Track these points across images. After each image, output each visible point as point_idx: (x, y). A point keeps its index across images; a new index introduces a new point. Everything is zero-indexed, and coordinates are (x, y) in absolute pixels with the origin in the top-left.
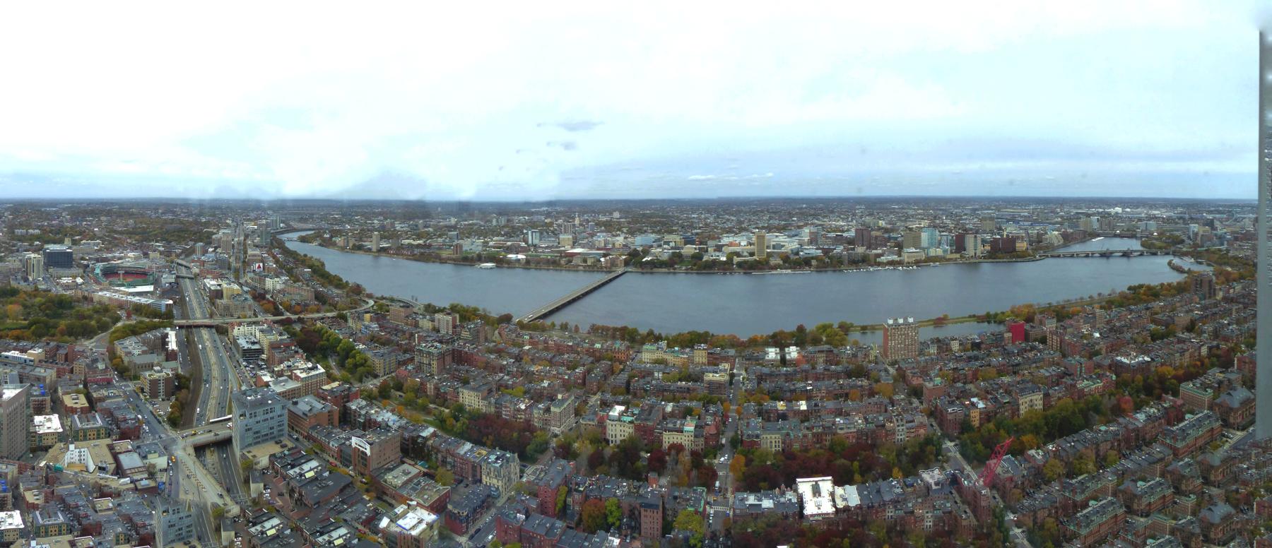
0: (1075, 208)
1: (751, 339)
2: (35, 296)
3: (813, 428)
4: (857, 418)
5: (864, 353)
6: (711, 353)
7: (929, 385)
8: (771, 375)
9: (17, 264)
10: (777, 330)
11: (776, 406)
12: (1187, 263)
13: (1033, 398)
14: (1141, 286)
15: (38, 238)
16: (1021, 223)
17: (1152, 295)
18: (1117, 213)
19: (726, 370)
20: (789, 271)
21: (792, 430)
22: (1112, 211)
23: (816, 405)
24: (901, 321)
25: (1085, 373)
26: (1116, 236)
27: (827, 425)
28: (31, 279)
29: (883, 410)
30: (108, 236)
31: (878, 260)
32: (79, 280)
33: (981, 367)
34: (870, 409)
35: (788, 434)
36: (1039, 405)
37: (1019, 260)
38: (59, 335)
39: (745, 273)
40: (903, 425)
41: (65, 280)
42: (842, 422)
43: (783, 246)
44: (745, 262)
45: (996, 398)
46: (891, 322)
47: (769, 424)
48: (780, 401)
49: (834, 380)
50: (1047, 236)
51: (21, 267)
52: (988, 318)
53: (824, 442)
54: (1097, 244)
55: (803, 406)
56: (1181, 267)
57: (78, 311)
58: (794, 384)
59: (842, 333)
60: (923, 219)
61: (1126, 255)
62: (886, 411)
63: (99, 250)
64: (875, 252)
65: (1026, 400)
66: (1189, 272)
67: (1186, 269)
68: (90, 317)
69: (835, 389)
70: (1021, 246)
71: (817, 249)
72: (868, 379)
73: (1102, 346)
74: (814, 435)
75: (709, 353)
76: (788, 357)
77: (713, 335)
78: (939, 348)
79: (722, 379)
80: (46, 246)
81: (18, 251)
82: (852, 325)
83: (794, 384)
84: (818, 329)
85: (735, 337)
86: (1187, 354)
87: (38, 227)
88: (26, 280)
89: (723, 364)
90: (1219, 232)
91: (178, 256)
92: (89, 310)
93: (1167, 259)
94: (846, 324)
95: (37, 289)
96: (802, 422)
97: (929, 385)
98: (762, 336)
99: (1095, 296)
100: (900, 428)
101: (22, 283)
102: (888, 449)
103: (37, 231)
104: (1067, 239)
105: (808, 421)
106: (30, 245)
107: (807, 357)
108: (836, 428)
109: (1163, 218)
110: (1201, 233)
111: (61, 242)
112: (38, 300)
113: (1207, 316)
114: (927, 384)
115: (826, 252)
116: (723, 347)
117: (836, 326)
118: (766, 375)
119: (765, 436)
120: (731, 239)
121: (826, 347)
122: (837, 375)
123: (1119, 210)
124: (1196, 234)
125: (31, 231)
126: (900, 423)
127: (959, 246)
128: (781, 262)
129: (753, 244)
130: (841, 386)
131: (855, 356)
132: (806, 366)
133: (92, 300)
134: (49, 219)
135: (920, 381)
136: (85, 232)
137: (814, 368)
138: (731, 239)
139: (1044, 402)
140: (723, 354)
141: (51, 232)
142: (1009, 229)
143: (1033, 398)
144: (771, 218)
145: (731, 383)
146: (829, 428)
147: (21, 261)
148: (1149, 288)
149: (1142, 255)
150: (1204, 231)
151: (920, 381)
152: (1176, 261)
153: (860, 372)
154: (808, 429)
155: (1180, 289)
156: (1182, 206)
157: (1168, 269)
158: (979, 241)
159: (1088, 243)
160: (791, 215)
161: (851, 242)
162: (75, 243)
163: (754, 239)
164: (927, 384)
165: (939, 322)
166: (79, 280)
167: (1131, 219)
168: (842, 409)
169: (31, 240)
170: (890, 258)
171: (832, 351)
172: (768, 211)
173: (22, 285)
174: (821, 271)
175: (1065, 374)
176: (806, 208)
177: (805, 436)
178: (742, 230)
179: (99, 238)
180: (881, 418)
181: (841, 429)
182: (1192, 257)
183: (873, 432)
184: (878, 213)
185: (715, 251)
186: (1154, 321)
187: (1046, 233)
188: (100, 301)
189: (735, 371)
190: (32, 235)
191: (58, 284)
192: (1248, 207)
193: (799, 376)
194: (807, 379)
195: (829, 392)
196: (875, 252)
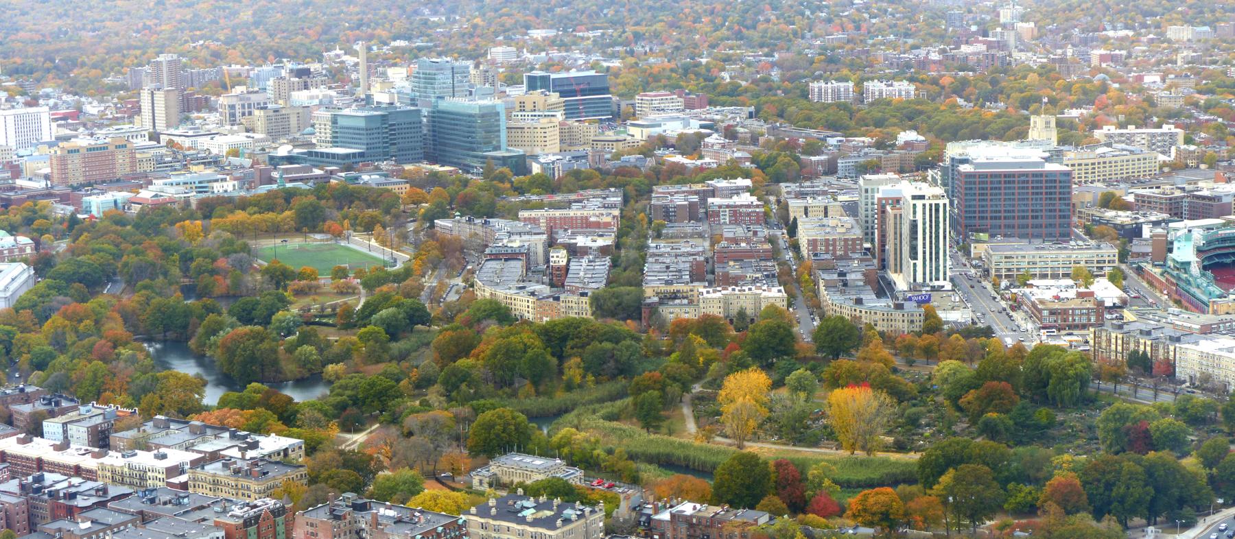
2: (930, 354)
9: (842, 226)
15: (910, 116)
28: (901, 282)
30: (1207, 108)
32: (1107, 292)
38: (1053, 508)
41: (1043, 291)
51: (858, 233)
57: (1122, 416)
63: (1176, 167)
68: (1175, 442)
80: (953, 150)
81: (831, 169)
87: (903, 71)
88: (883, 288)
92: (1164, 411)
95: (932, 325)
101: (870, 298)
103: (903, 89)
106: (879, 145)
111: (1015, 131)
112: (947, 366)
125: (875, 87)
133: (1169, 369)
134: (942, 37)
136: (1104, 89)
141: (960, 88)
147: (851, 209)
162: (1068, 134)
166: (1107, 292)
169: (879, 123)
173: (874, 310)
179: (1170, 116)
188: (1206, 378)
190: (880, 102)
191: (1017, 304)
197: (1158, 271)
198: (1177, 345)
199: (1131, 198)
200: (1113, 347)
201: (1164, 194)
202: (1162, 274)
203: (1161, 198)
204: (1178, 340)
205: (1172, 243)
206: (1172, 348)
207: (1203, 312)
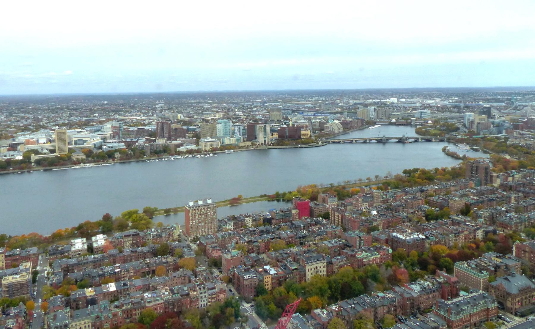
0: (354, 99)
1: (54, 234)
3: (123, 305)
4: (164, 291)
5: (168, 233)
6: (10, 256)
7: (227, 256)
8: (79, 264)
10: (83, 221)
11: (84, 294)
12: (463, 150)
13: (317, 265)
14: (416, 170)
16: (305, 113)
17: (426, 179)
18: (392, 103)
19: (27, 270)
20: (93, 165)
21: (101, 312)
22: (388, 101)
23: (125, 285)
24: (200, 203)
25: (364, 246)
26: (391, 124)
27: (135, 300)
29: (187, 281)
31: (178, 149)
33: (272, 239)
34: (175, 281)
35: (98, 317)
36: (323, 271)
37: (304, 146)
39: (45, 170)
40: (205, 293)
42: (150, 296)
43: (85, 141)
44: (45, 159)
45: (286, 265)
46: (191, 204)
47: (77, 312)
48: (88, 287)
49: (141, 260)
50: (328, 125)
52: (277, 197)
53: (134, 317)
54: (374, 132)
55: (112, 287)
56: (456, 154)
58: (102, 269)
59: (146, 217)
60: (218, 112)
61: (401, 141)
62: (190, 282)
64: (175, 142)
65: (312, 267)
66: (464, 158)
67: (461, 156)
69: (142, 268)
70: (306, 133)
71: (120, 142)
72: (172, 256)
73: (379, 222)
74: (124, 312)
75: (6, 256)
76: (95, 245)
77: (10, 237)
78: (235, 224)
79: (24, 279)
82: (156, 210)
83: (102, 269)
84: (124, 215)
85: (36, 235)
86: (462, 236)
89: (24, 264)
90: (497, 120)
93: (442, 145)
94: (150, 209)
96: (112, 302)
97: (227, 256)
98: (67, 229)
99: (373, 178)
100: (203, 295)
102: (192, 315)
104: (347, 127)
105: (118, 300)
107: (114, 242)
108: (145, 302)
109: (438, 107)
110: (477, 121)
113: (482, 202)
114: (225, 255)
115: (129, 145)
116: (22, 247)
117: (141, 211)
118: (73, 265)
119: (74, 324)
120: (27, 137)
121: (132, 231)
122: (144, 256)
123: (394, 100)
124: (472, 122)
126: (203, 291)
127: (250, 134)
128: (84, 157)
129: (54, 141)
130: (148, 265)
131: (160, 236)
132: (114, 251)
135: (219, 253)
137: (121, 252)
138: (27, 137)
139: (327, 269)
140: (24, 254)
142: (294, 119)
143: (317, 265)
144: (71, 115)
145: (34, 281)
146: (138, 303)
148: (424, 172)
149: (416, 141)
150: (480, 119)
151: (219, 253)
152: (451, 148)
153: (166, 251)
154: (118, 307)
155: (455, 174)
156: (457, 95)
157: (442, 155)
158: (268, 130)
159: (366, 130)
160: (92, 111)
161: (152, 134)
163: (54, 136)
164: (225, 255)
165: (235, 202)
167: (406, 109)
168: (149, 284)
170: (189, 147)
171: (138, 234)
172: (68, 108)
174: (124, 163)
175: (346, 246)
176: (107, 104)
177: (115, 315)
178: (39, 127)
180: (186, 288)
181: (149, 302)
182: (468, 144)
183: (179, 301)
184: (177, 108)
185: (9, 150)
186: (428, 203)
187: (328, 122)
189: (38, 268)
192: (531, 94)
193: (107, 261)
194: (115, 263)
195: (136, 272)
196: (175, 142)
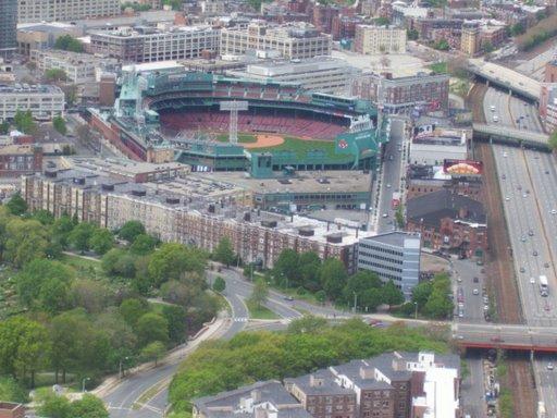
91: (484, 49)
197: (104, 116)
198: (109, 194)
199: (87, 40)
200: (45, 196)
201: (121, 35)
202: (108, 120)
203: (117, 40)
204: (110, 189)
205: (120, 87)
206: (104, 197)
207: (144, 159)
